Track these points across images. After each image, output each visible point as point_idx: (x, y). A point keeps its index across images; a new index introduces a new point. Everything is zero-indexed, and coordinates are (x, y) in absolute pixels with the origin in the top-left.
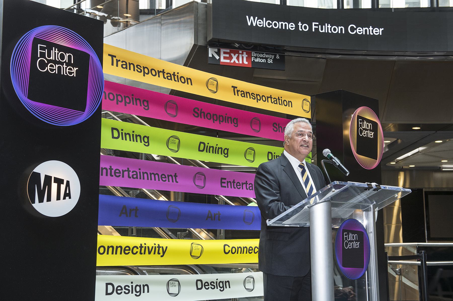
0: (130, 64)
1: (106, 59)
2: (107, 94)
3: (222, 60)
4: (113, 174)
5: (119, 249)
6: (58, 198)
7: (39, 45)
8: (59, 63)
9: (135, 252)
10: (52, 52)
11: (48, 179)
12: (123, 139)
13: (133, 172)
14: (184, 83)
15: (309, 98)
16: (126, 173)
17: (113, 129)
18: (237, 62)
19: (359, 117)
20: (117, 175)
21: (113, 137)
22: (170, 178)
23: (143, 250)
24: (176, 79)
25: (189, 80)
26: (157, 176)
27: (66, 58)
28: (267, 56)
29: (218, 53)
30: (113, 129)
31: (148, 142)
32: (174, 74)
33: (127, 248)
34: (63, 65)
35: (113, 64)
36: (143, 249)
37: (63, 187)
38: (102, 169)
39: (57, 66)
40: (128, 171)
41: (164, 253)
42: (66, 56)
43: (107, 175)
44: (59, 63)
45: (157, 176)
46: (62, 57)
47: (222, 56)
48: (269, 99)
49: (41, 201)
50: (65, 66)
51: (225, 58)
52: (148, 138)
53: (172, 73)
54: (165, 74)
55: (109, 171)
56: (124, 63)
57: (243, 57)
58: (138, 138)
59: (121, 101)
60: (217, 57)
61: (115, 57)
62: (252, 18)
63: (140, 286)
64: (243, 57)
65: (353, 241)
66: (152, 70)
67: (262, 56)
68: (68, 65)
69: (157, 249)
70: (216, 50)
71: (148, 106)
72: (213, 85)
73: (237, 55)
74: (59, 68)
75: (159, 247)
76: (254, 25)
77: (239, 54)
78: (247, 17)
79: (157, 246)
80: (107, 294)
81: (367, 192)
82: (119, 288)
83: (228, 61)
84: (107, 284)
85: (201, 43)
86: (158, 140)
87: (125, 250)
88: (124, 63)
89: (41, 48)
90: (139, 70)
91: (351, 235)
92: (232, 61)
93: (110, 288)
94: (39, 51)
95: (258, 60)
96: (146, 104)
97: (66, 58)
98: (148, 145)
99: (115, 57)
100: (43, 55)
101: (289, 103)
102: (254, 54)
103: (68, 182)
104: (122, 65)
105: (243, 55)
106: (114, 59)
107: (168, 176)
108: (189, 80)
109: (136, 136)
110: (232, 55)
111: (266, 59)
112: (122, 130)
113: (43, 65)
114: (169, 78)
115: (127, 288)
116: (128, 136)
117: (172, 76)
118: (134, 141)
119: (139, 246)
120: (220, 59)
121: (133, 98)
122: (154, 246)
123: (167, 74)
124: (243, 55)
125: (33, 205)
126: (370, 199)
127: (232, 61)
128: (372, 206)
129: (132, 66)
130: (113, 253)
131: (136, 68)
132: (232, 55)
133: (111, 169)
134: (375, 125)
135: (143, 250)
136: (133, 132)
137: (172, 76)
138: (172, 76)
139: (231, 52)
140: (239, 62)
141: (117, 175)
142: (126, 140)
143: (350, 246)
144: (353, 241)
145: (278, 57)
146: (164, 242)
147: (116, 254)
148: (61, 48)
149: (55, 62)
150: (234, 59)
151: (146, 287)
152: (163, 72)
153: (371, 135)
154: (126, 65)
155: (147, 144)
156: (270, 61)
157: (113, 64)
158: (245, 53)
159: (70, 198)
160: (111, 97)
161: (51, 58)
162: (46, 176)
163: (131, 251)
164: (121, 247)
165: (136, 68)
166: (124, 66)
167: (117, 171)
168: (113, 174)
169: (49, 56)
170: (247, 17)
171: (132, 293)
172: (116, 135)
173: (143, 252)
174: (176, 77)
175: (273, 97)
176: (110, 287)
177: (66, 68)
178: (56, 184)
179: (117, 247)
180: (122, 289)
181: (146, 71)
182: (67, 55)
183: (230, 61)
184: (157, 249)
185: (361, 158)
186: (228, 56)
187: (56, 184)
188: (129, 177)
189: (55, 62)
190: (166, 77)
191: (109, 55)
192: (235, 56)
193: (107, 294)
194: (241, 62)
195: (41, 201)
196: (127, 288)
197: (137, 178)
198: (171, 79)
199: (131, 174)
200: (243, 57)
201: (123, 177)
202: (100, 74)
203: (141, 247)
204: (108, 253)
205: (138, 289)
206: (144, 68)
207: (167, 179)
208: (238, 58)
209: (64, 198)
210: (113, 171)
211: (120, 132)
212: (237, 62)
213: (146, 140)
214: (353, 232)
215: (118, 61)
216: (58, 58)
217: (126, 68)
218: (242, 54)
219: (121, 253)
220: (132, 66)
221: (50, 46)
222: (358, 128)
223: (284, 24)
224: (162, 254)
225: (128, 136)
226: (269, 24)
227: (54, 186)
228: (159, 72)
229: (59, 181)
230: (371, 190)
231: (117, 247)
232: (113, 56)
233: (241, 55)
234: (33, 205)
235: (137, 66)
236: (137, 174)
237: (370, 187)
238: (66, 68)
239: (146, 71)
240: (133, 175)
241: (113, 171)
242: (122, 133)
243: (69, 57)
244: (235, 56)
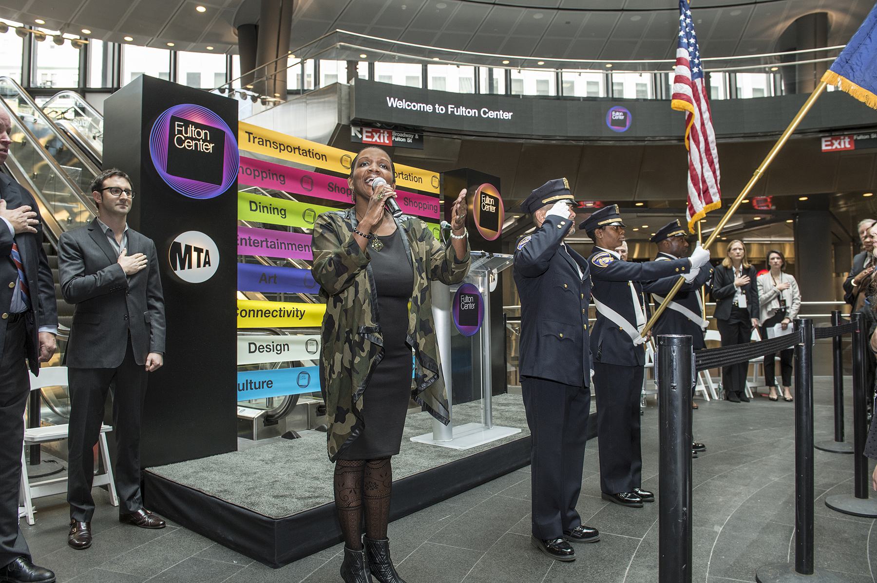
0: (266, 141)
1: (242, 135)
2: (244, 169)
3: (365, 139)
4: (252, 244)
5: (260, 312)
6: (199, 266)
7: (176, 123)
8: (196, 139)
9: (274, 315)
10: (189, 129)
11: (188, 248)
12: (260, 212)
13: (271, 242)
14: (319, 159)
15: (438, 175)
16: (264, 243)
17: (251, 202)
19: (482, 193)
20: (256, 245)
21: (251, 210)
22: (307, 247)
23: (282, 313)
24: (311, 156)
25: (324, 157)
26: (294, 246)
27: (203, 135)
28: (407, 136)
29: (361, 132)
30: (251, 202)
31: (285, 214)
32: (309, 151)
33: (268, 312)
34: (199, 141)
35: (249, 141)
36: (282, 312)
37: (203, 255)
38: (242, 239)
39: (194, 142)
40: (267, 241)
41: (302, 316)
42: (203, 133)
43: (246, 245)
44: (196, 139)
45: (294, 246)
46: (199, 134)
47: (365, 135)
48: (401, 175)
49: (183, 268)
50: (201, 143)
51: (367, 137)
52: (285, 210)
53: (307, 150)
54: (301, 151)
55: (248, 241)
56: (261, 140)
57: (384, 136)
58: (276, 210)
59: (258, 176)
60: (360, 136)
61: (252, 134)
62: (392, 99)
63: (281, 345)
65: (469, 303)
66: (287, 146)
67: (402, 135)
68: (205, 141)
69: (296, 312)
70: (359, 129)
71: (284, 180)
72: (347, 161)
73: (378, 134)
74: (196, 144)
75: (297, 311)
76: (395, 106)
77: (381, 133)
78: (388, 98)
79: (295, 309)
80: (250, 352)
81: (482, 260)
82: (261, 347)
83: (370, 140)
84: (250, 344)
85: (345, 122)
86: (295, 213)
87: (265, 313)
88: (261, 140)
89: (179, 126)
90: (275, 147)
91: (467, 297)
92: (374, 140)
93: (253, 348)
94: (176, 128)
95: (398, 139)
96: (282, 178)
97: (203, 135)
98: (285, 217)
99: (252, 134)
100: (180, 132)
101: (419, 180)
102: (394, 133)
103: (207, 251)
104: (259, 142)
106: (251, 136)
107: (305, 246)
108: (324, 157)
109: (274, 209)
110: (374, 134)
111: (406, 138)
112: (260, 203)
113: (181, 142)
114: (305, 154)
115: (268, 347)
116: (265, 209)
117: (308, 153)
118: (271, 213)
119: (278, 309)
120: (362, 138)
121: (269, 173)
122: (293, 310)
123: (303, 150)
125: (175, 272)
126: (484, 266)
127: (374, 140)
128: (486, 272)
129: (268, 143)
130: (254, 316)
131: (272, 145)
132: (374, 134)
133: (250, 239)
134: (496, 200)
135: (282, 313)
136: (271, 205)
137: (308, 153)
138: (307, 153)
139: (373, 131)
140: (380, 140)
141: (256, 245)
142: (264, 212)
143: (466, 307)
144: (469, 303)
145: (417, 137)
146: (300, 306)
147: (257, 316)
148: (197, 126)
149: (192, 139)
150: (376, 138)
151: (286, 346)
152: (299, 148)
153: (493, 209)
154: (263, 141)
155: (284, 216)
156: (410, 141)
157: (249, 141)
158: (386, 132)
159: (210, 266)
160: (249, 172)
161: (188, 135)
162: (186, 246)
163: (271, 315)
164: (261, 311)
165: (272, 145)
166: (261, 143)
167: (256, 241)
168: (252, 244)
169: (186, 133)
170: (388, 98)
171: (273, 351)
172: (254, 207)
173: (282, 315)
174: (311, 153)
175: (404, 173)
176: (253, 347)
177: (203, 144)
178: (196, 253)
179: (258, 311)
180: (264, 348)
181: (282, 148)
182: (204, 132)
184: (296, 312)
185: (484, 231)
186: (370, 135)
187: (196, 253)
188: (268, 247)
189: (192, 139)
190: (301, 153)
191: (246, 132)
193: (250, 352)
194: (382, 141)
195: (183, 268)
196: (268, 347)
197: (275, 247)
198: (306, 155)
199: (269, 244)
200: (384, 136)
201: (262, 247)
202: (235, 150)
203: (281, 310)
204: (249, 316)
205: (279, 348)
206: (280, 145)
207: (304, 249)
208: (379, 137)
209: (204, 266)
210: (252, 241)
211: (258, 205)
212: (378, 141)
213: (283, 212)
214: (470, 295)
215: (254, 138)
216: (195, 136)
217: (263, 144)
218: (384, 133)
219: (262, 316)
220: (268, 143)
221: (187, 123)
222: (481, 203)
223: (422, 105)
224: (300, 317)
225: (265, 209)
226: (409, 106)
227: (194, 255)
228: (295, 149)
229: (199, 251)
230: (485, 258)
231: (258, 311)
232: (250, 134)
234: (175, 272)
235: (273, 142)
236: (275, 244)
237: (483, 255)
238: (203, 144)
239: (282, 148)
240: (271, 245)
241: (252, 241)
242: (260, 206)
243: (206, 134)
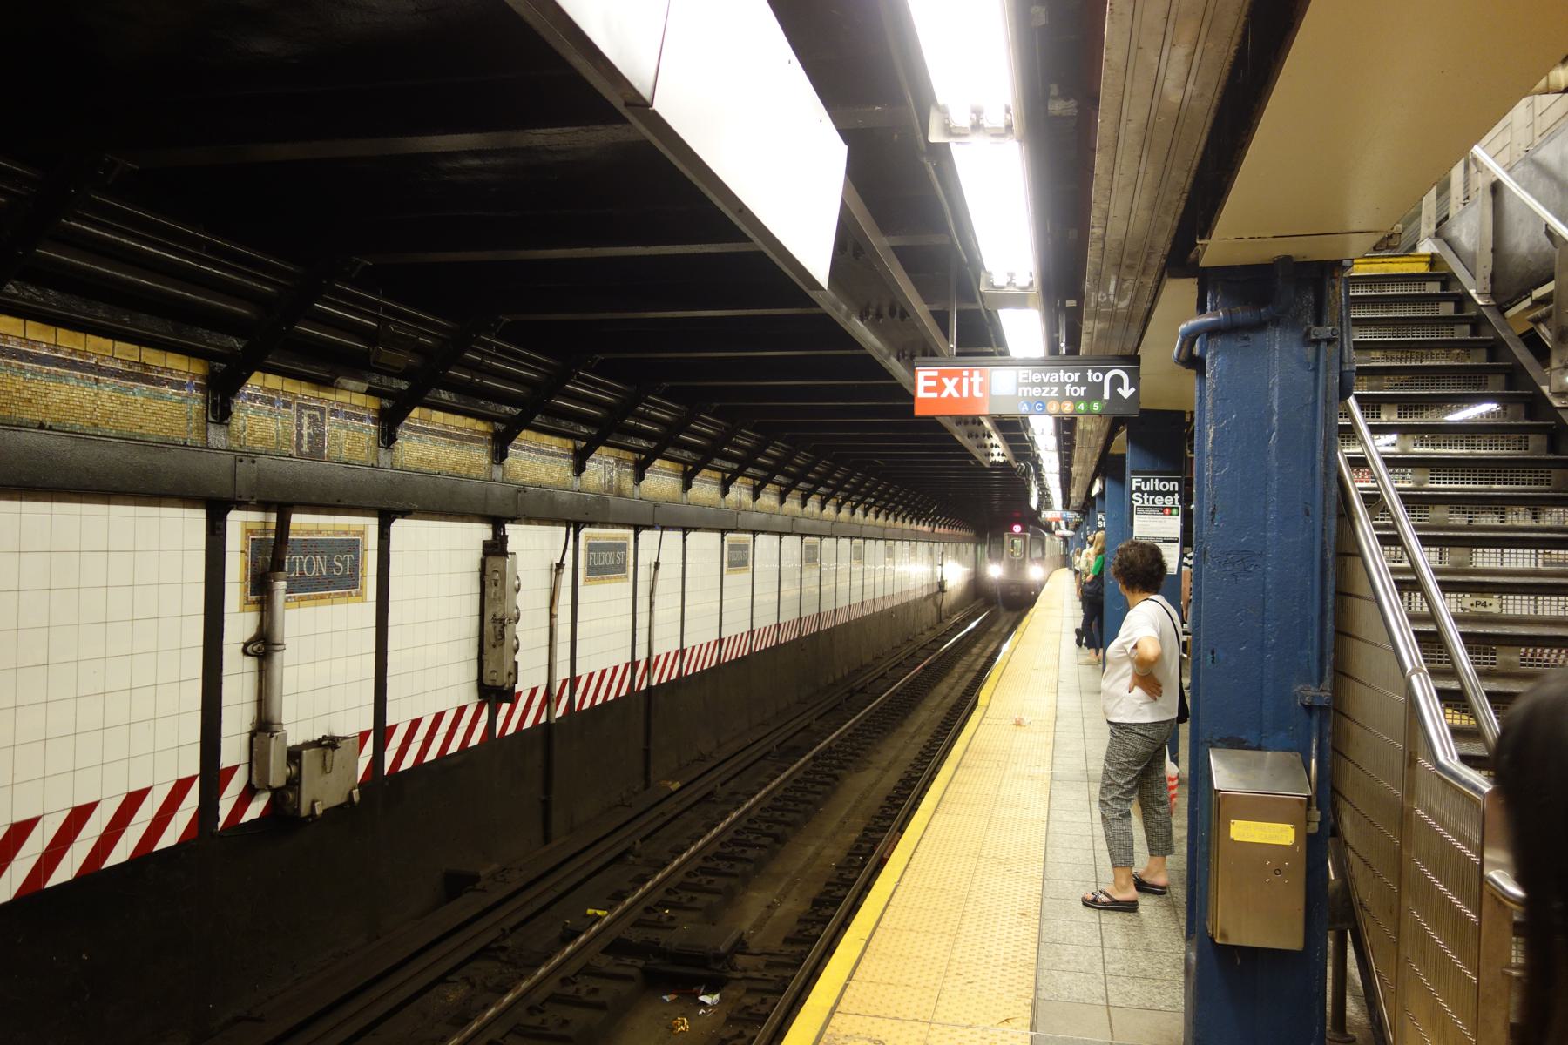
51: (927, 389)
73: (955, 380)
83: (934, 395)
92: (944, 395)
105: (972, 379)
110: (945, 380)
127: (944, 395)
132: (945, 380)
139: (942, 374)
183: (939, 395)
186: (933, 383)
212: (955, 395)
218: (971, 375)
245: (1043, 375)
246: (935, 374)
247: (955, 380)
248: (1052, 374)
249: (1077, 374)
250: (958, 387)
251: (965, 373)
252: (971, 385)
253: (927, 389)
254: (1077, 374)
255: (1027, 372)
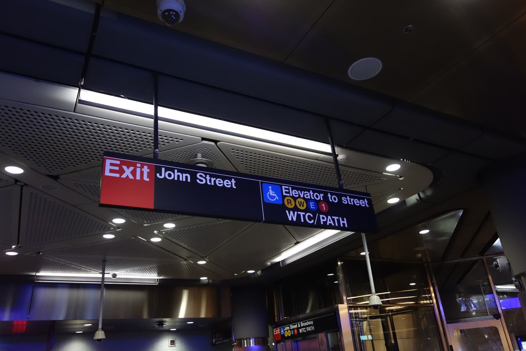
18: (131, 177)
51: (111, 171)
64: (143, 171)
73: (132, 168)
83: (117, 175)
92: (124, 176)
105: (143, 170)
110: (125, 168)
124: (143, 169)
127: (124, 176)
132: (125, 168)
139: (123, 163)
150: (128, 172)
183: (121, 175)
186: (117, 168)
192: (128, 169)
212: (131, 177)
218: (142, 167)
233: (140, 169)
244: (128, 169)
245: (299, 191)
246: (118, 162)
247: (132, 168)
248: (305, 192)
249: (322, 195)
250: (134, 173)
251: (139, 165)
252: (142, 173)
253: (111, 171)
254: (322, 195)
255: (288, 187)
